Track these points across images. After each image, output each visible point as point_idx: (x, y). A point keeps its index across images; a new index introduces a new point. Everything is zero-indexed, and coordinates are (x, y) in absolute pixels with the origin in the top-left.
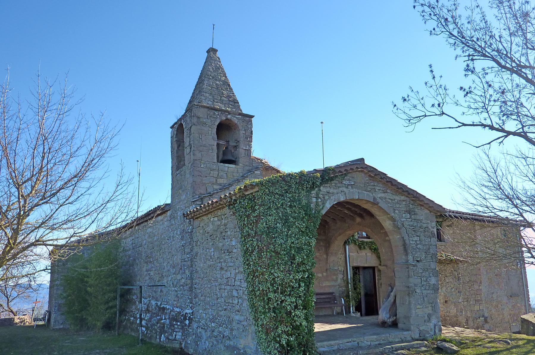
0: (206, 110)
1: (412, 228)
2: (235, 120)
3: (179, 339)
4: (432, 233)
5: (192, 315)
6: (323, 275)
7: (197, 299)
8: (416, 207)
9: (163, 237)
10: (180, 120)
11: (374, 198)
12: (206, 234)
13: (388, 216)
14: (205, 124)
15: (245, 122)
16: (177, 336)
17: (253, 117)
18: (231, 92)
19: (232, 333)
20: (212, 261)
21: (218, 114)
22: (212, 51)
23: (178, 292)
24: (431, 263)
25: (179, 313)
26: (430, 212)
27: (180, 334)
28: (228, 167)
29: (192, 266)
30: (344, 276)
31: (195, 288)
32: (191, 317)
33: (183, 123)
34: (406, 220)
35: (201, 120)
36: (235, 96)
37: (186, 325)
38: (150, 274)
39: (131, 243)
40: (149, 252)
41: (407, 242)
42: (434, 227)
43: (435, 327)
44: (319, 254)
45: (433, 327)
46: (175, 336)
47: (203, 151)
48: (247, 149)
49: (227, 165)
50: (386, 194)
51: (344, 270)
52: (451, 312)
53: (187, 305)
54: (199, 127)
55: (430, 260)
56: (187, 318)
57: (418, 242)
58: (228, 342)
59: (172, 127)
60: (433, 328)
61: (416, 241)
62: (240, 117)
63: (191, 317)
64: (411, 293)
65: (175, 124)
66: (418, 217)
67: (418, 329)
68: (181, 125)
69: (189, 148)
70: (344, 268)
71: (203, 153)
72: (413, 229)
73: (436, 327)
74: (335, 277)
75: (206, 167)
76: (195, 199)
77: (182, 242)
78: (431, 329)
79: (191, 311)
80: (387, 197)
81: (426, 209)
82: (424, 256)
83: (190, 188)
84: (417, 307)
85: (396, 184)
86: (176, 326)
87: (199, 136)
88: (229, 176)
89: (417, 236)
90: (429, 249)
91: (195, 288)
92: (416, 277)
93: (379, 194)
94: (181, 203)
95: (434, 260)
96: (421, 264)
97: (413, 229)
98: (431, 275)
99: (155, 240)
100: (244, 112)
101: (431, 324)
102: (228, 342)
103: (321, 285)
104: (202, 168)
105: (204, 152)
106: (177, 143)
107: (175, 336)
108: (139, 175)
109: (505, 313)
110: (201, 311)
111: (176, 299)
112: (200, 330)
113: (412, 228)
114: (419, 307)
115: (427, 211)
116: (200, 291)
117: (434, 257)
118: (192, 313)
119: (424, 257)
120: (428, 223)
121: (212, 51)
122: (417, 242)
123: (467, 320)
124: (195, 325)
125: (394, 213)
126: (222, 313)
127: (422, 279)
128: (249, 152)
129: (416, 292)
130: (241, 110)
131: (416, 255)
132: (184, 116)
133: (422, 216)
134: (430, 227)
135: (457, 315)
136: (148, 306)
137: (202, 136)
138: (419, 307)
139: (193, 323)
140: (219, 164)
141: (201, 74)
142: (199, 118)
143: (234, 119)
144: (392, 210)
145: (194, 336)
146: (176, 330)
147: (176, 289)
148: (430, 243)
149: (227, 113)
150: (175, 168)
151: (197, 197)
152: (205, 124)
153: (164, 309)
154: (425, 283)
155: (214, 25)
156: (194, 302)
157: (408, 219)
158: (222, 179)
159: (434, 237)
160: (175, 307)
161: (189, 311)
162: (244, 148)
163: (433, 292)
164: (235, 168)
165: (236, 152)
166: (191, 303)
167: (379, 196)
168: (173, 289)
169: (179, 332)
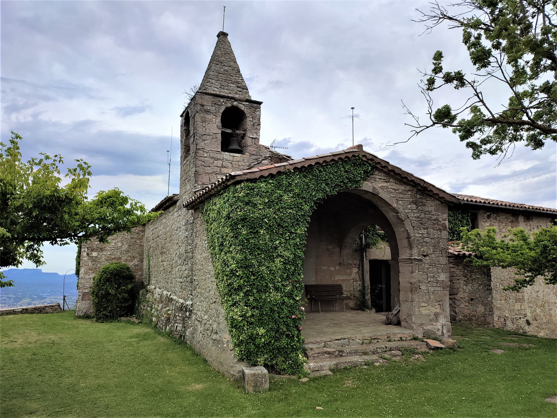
0: (211, 97)
1: (419, 219)
2: (242, 107)
3: (180, 330)
4: (443, 225)
5: (192, 307)
6: (335, 269)
7: (195, 292)
8: (424, 197)
9: (173, 227)
10: (187, 108)
11: (374, 188)
12: (203, 226)
13: (391, 207)
14: (208, 112)
15: (253, 109)
16: (178, 328)
17: (260, 103)
18: (240, 78)
19: (219, 326)
20: (207, 253)
21: (223, 101)
22: (222, 35)
23: (183, 284)
24: (441, 258)
25: (182, 304)
26: (442, 203)
27: (181, 325)
28: (234, 156)
29: (193, 257)
30: (359, 270)
31: (195, 280)
32: (191, 309)
33: (189, 111)
34: (412, 212)
35: (205, 107)
36: (244, 82)
37: (186, 317)
38: (164, 264)
39: (151, 233)
40: (163, 242)
41: (412, 235)
42: (446, 219)
43: (443, 328)
44: (332, 247)
45: (440, 328)
46: (177, 327)
47: (207, 140)
48: (254, 137)
49: (232, 154)
50: (389, 184)
51: (359, 264)
52: (478, 312)
53: (189, 297)
54: (202, 115)
55: (438, 255)
56: (188, 310)
57: (425, 236)
58: (214, 337)
59: (182, 116)
60: (441, 329)
61: (423, 234)
62: (248, 103)
63: (191, 309)
64: (414, 289)
65: (184, 112)
66: (426, 208)
67: (422, 329)
68: (188, 113)
69: (193, 136)
70: (360, 262)
71: (206, 142)
72: (420, 221)
73: (444, 327)
74: (349, 271)
75: (209, 156)
76: (197, 190)
77: (186, 233)
78: (438, 330)
79: (191, 303)
80: (390, 187)
81: (436, 200)
82: (432, 250)
83: (193, 178)
84: (421, 305)
85: (399, 172)
86: (178, 318)
87: (203, 124)
88: (235, 166)
89: (424, 229)
90: (439, 242)
91: (195, 280)
92: (421, 273)
93: (380, 183)
94: (186, 193)
95: (444, 255)
96: (427, 258)
97: (420, 221)
98: (440, 271)
99: (167, 230)
100: (253, 99)
101: (438, 324)
102: (214, 337)
103: (333, 279)
104: (204, 158)
105: (207, 141)
106: (185, 132)
107: (177, 327)
108: (170, 165)
109: (553, 313)
110: (198, 303)
111: (181, 290)
112: (196, 322)
113: (419, 219)
114: (424, 304)
115: (438, 201)
116: (197, 283)
117: (444, 252)
118: (192, 304)
119: (432, 251)
120: (438, 215)
121: (222, 35)
122: (424, 235)
123: (505, 320)
124: (194, 317)
125: (397, 203)
126: (212, 306)
127: (429, 275)
128: (257, 139)
129: (420, 289)
130: (250, 97)
131: (422, 249)
132: (190, 104)
133: (432, 207)
134: (440, 220)
135: (485, 314)
136: (161, 296)
137: (205, 124)
138: (424, 304)
139: (193, 315)
140: (223, 153)
141: (211, 59)
142: (203, 106)
143: (240, 106)
144: (394, 200)
145: (192, 328)
146: (177, 321)
147: (181, 280)
148: (440, 236)
149: (233, 100)
150: (183, 158)
151: (199, 187)
152: (208, 112)
153: (172, 299)
154: (432, 280)
155: (225, 7)
156: (193, 294)
157: (413, 211)
158: (227, 169)
159: (445, 230)
160: (180, 298)
161: (189, 303)
162: (251, 136)
163: (442, 290)
164: (241, 157)
165: (244, 141)
166: (192, 295)
167: (380, 185)
168: (179, 279)
169: (180, 323)
